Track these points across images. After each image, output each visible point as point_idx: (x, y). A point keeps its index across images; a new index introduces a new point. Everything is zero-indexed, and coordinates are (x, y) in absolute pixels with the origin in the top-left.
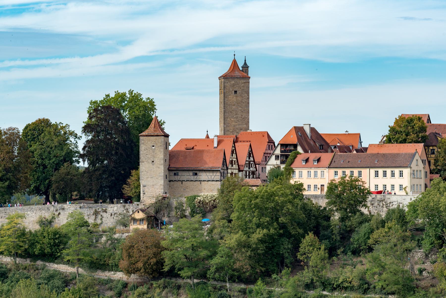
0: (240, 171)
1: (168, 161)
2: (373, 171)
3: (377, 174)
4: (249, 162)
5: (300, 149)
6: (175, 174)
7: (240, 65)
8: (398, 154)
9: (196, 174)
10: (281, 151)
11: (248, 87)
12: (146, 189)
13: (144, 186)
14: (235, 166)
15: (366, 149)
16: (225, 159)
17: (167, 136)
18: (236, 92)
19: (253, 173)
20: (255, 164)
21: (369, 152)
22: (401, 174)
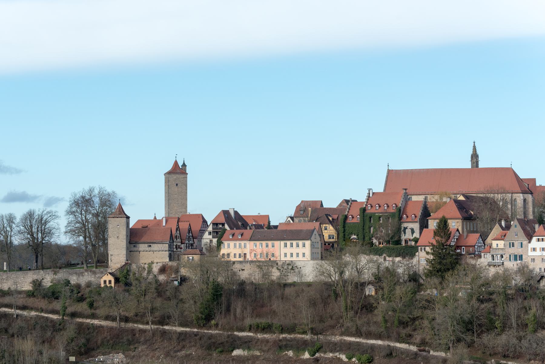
0: (182, 243)
1: (129, 236)
2: (283, 243)
3: (286, 245)
4: (189, 237)
5: (226, 227)
6: (134, 246)
7: (180, 164)
8: (301, 230)
9: (150, 246)
10: (213, 229)
11: (186, 181)
12: (113, 258)
13: (112, 255)
14: (179, 240)
15: (276, 227)
16: (171, 235)
17: (128, 218)
18: (177, 185)
19: (192, 245)
20: (193, 239)
21: (279, 229)
22: (304, 245)
